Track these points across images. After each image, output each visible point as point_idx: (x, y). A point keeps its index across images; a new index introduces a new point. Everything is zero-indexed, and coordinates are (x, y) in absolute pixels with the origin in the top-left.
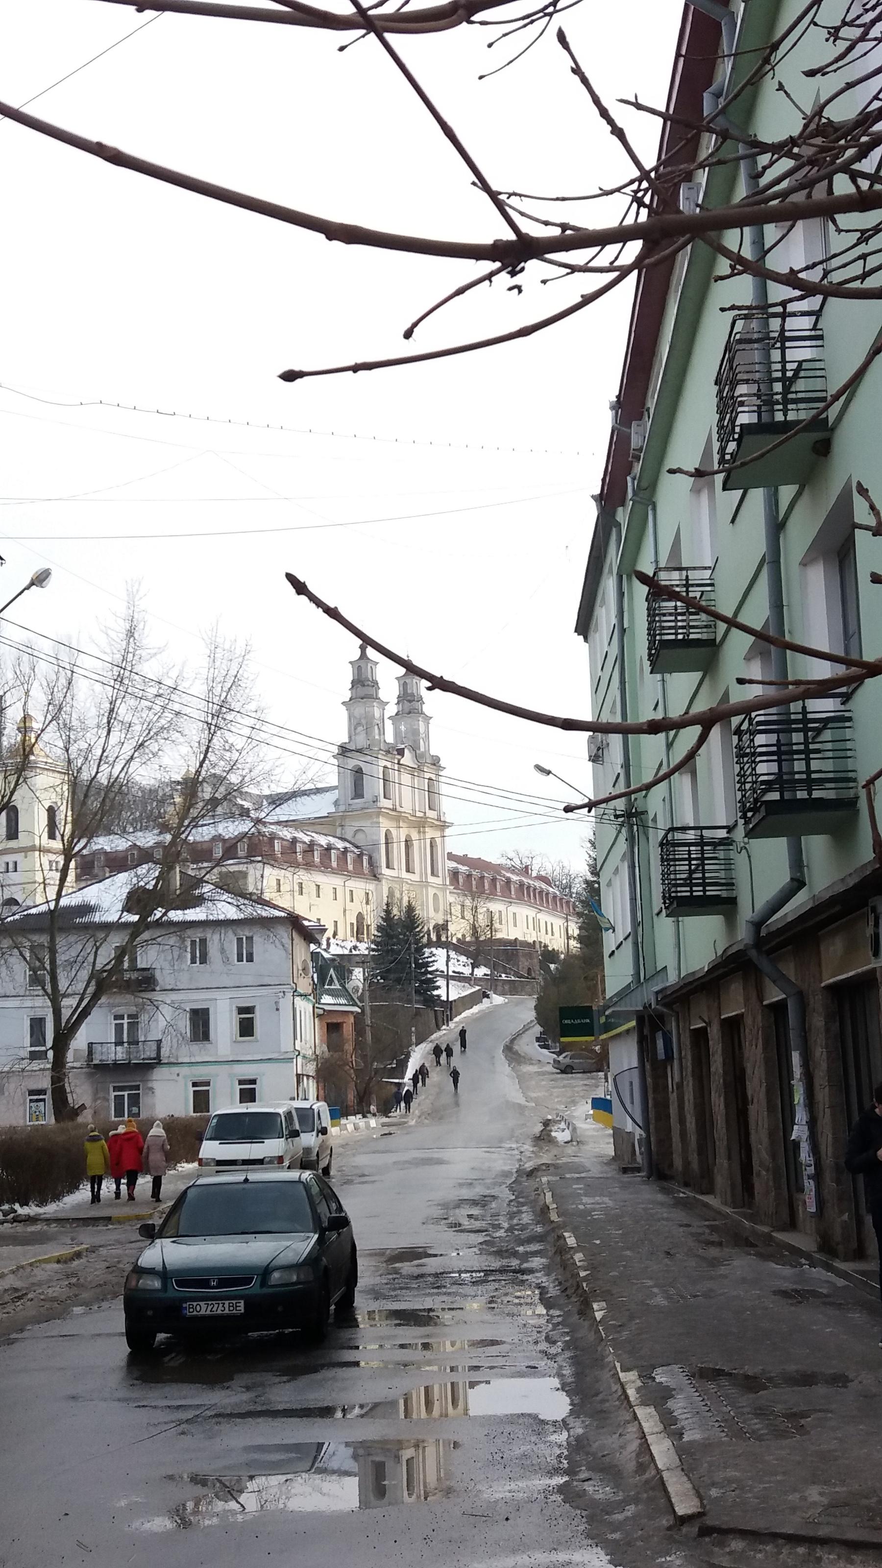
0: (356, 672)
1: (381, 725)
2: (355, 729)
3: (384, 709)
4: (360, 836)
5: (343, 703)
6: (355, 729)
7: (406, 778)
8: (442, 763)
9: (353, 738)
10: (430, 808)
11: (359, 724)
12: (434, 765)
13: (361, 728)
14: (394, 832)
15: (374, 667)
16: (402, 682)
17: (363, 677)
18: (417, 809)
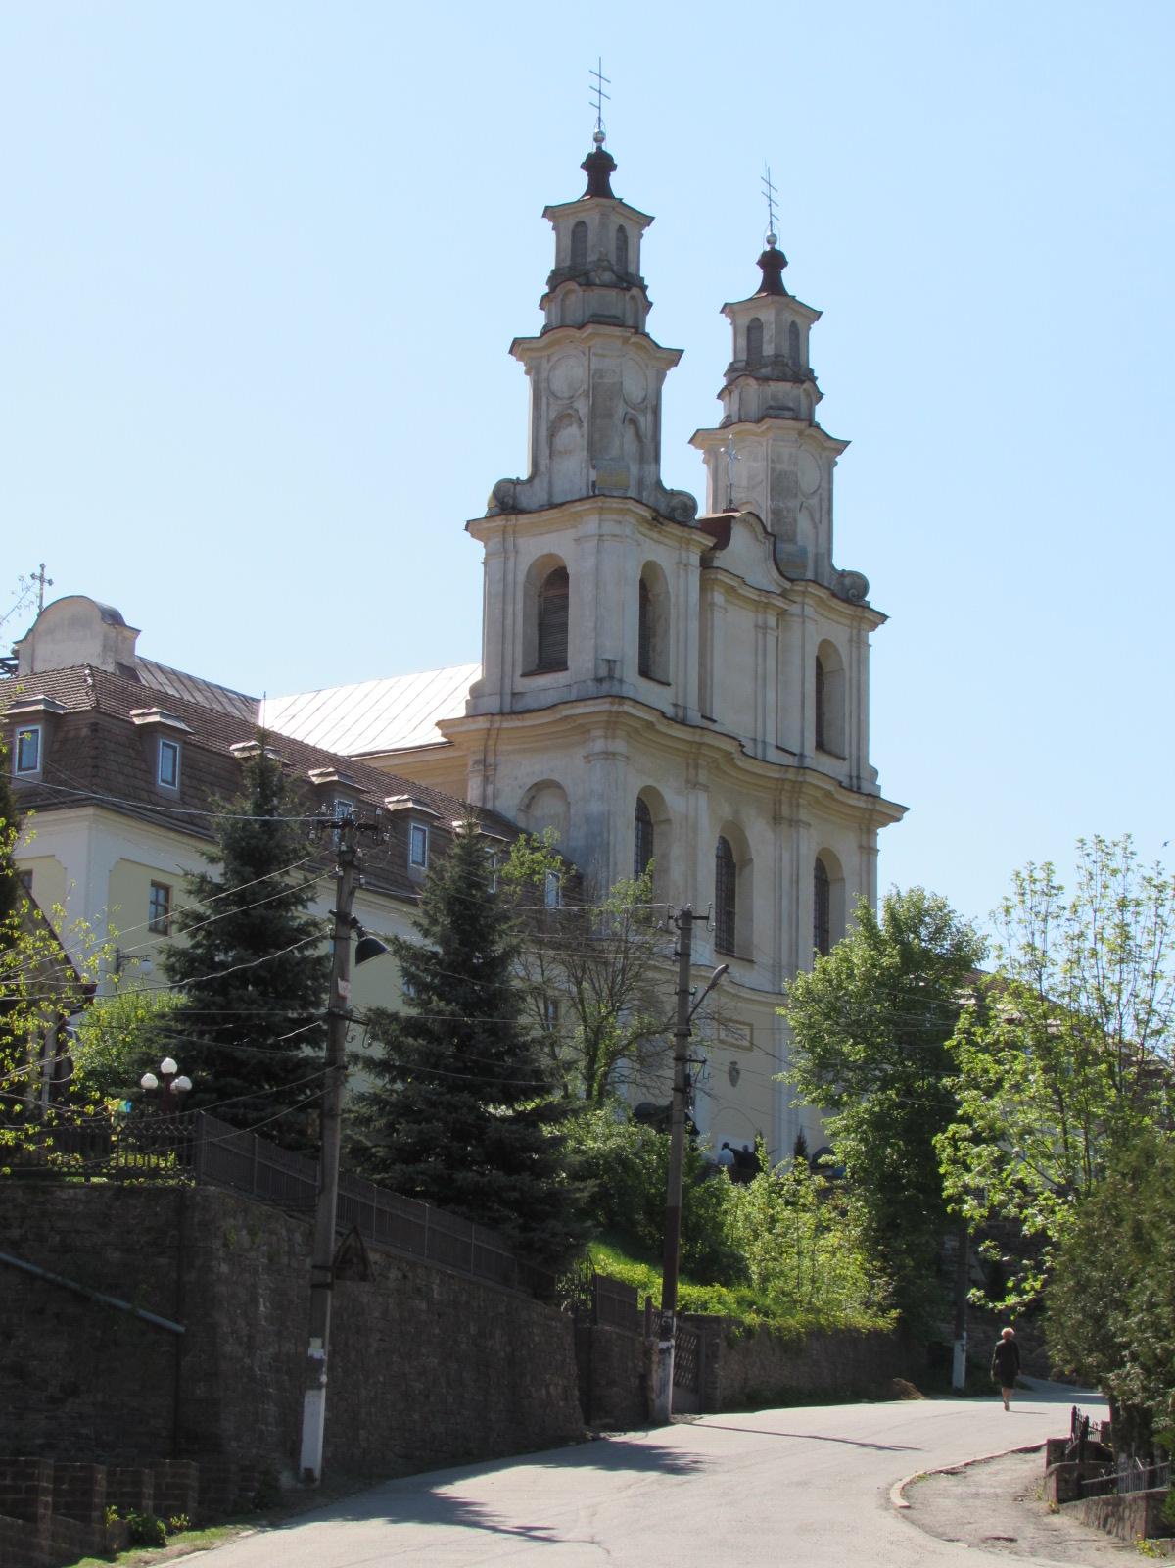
0: (567, 242)
1: (645, 422)
2: (552, 436)
3: (660, 378)
4: (548, 805)
5: (518, 346)
6: (552, 436)
7: (735, 623)
8: (875, 599)
9: (544, 462)
10: (820, 746)
11: (566, 416)
12: (847, 600)
13: (573, 430)
14: (676, 801)
15: (630, 232)
16: (744, 321)
17: (592, 257)
18: (771, 739)
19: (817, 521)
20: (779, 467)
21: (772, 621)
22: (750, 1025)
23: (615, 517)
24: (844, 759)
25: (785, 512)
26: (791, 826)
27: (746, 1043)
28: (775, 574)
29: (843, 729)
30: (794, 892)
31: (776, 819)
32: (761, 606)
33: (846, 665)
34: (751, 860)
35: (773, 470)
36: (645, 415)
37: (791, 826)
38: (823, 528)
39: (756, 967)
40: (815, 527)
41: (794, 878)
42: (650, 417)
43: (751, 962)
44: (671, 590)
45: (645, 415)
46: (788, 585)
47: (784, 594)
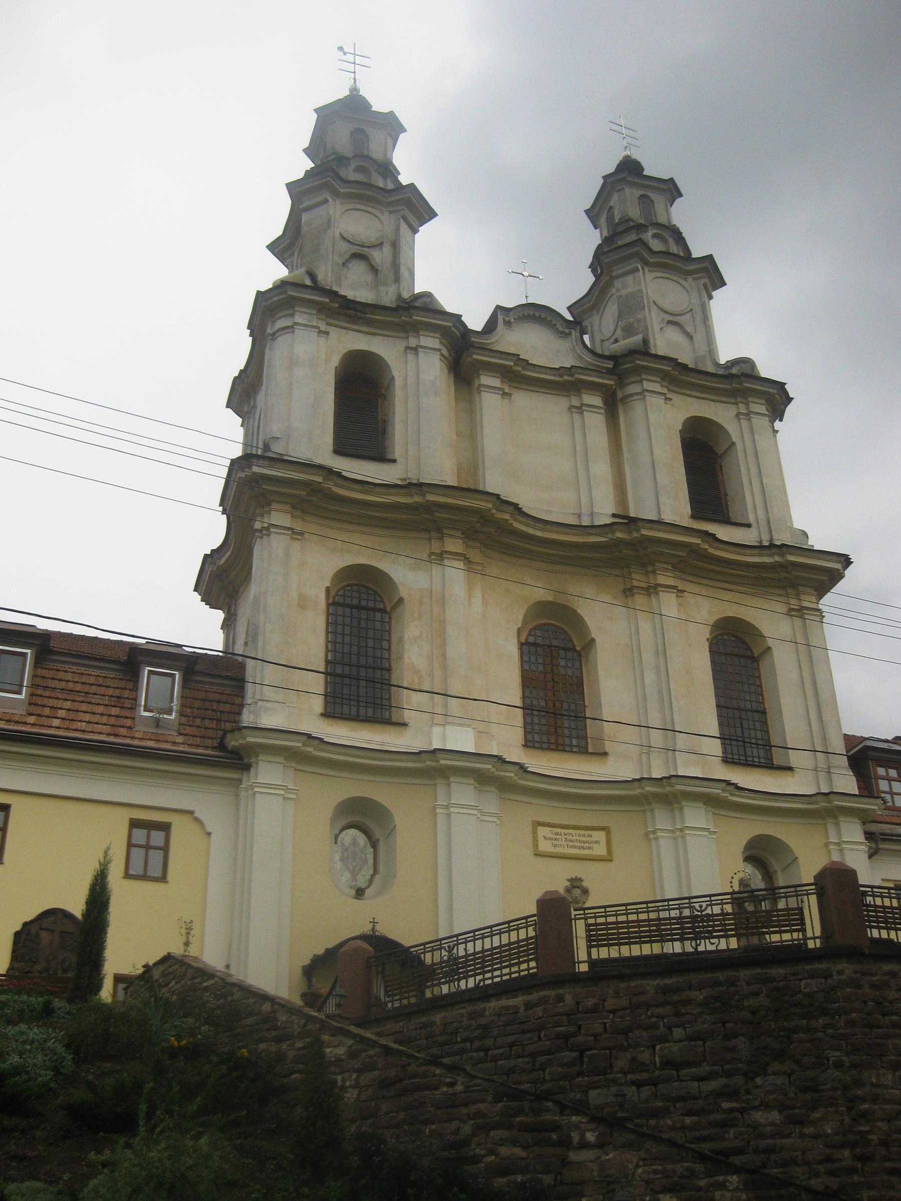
19: (690, 329)
20: (624, 292)
21: (597, 401)
22: (606, 829)
23: (286, 312)
24: (749, 526)
25: (636, 325)
26: (649, 595)
27: (600, 850)
28: (588, 358)
29: (744, 497)
30: (662, 668)
31: (628, 592)
32: (563, 383)
33: (735, 437)
34: (593, 640)
35: (619, 297)
36: (381, 250)
37: (649, 595)
38: (699, 337)
39: (611, 759)
40: (691, 338)
41: (660, 648)
42: (387, 249)
43: (605, 754)
44: (395, 373)
45: (381, 250)
46: (610, 365)
47: (610, 372)
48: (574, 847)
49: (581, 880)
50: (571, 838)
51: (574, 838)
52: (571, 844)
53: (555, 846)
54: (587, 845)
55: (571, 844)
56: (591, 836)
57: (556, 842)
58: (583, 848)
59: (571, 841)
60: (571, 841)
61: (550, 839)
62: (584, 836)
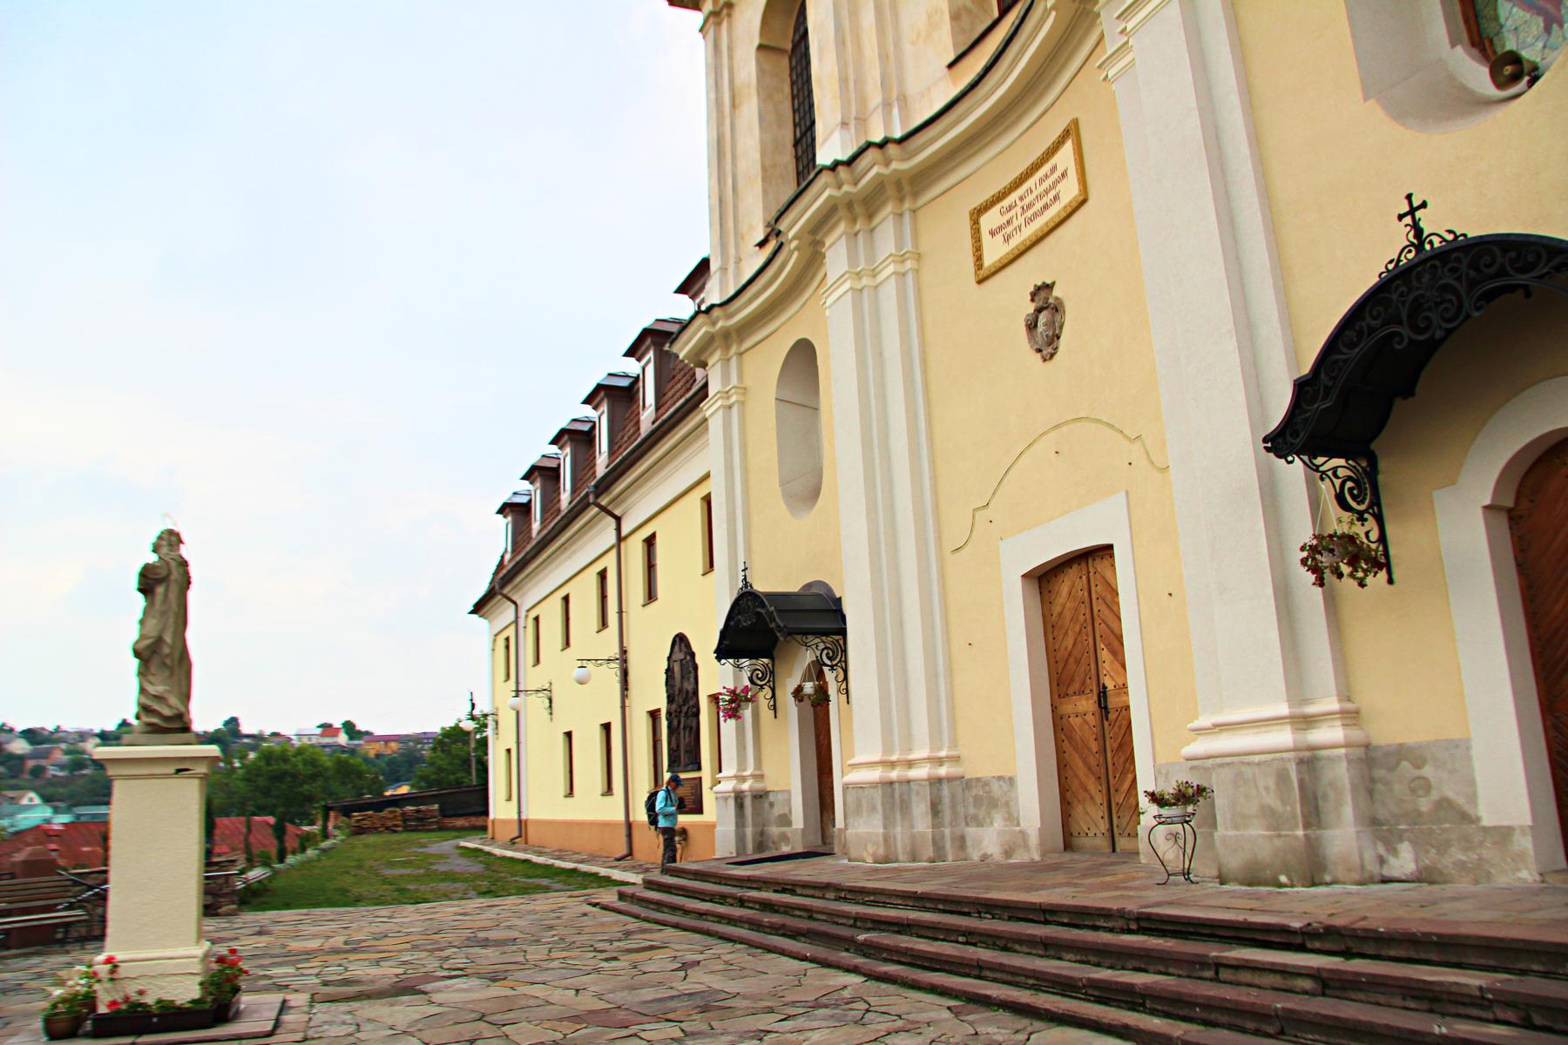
22: (1071, 132)
48: (1036, 215)
49: (1049, 287)
50: (1027, 201)
51: (1035, 193)
52: (1029, 213)
53: (1007, 239)
54: (1051, 195)
55: (1029, 213)
56: (1054, 169)
57: (1009, 229)
58: (1046, 207)
59: (1030, 206)
60: (1030, 206)
61: (1001, 228)
62: (1046, 176)
